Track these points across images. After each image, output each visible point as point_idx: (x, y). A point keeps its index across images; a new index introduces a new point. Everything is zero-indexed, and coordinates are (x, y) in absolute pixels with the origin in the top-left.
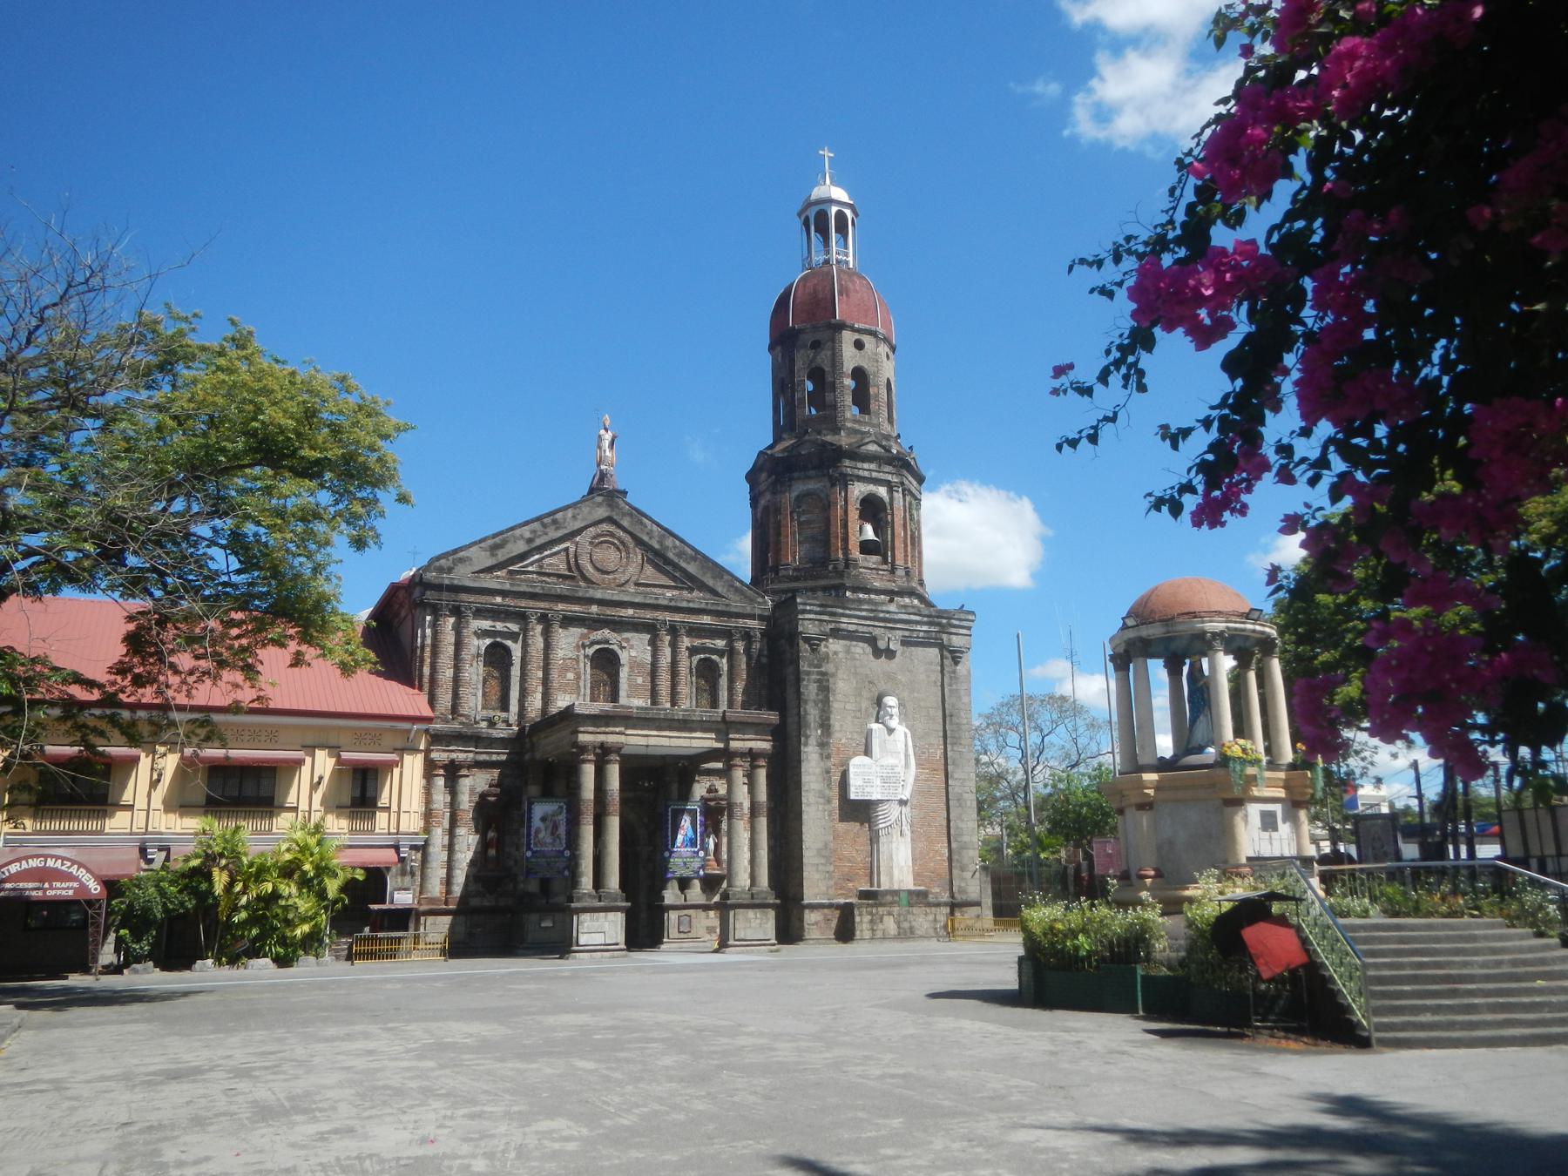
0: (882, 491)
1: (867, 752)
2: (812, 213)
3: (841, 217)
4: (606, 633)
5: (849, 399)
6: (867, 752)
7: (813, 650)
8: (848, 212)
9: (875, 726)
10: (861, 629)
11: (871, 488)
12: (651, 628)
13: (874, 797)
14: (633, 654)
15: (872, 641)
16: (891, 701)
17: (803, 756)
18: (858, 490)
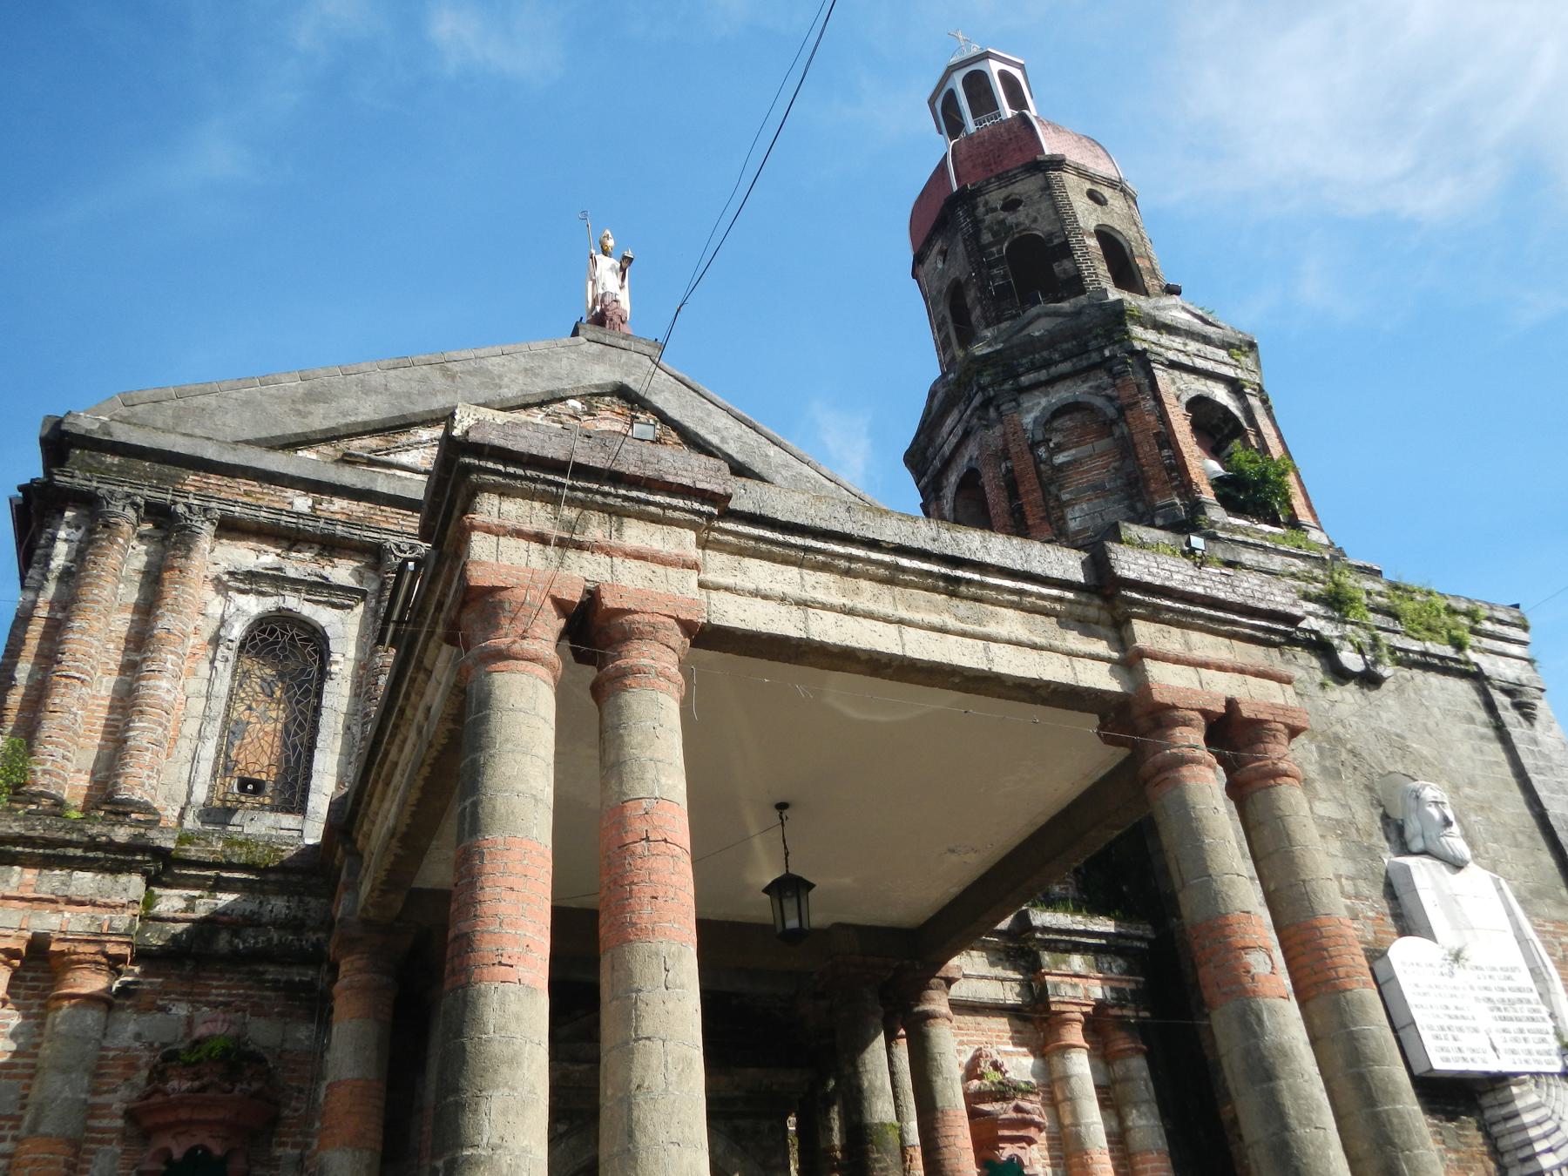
0: (1221, 395)
5: (1102, 269)
8: (1017, 73)
9: (1410, 861)
13: (1493, 1065)
15: (1322, 648)
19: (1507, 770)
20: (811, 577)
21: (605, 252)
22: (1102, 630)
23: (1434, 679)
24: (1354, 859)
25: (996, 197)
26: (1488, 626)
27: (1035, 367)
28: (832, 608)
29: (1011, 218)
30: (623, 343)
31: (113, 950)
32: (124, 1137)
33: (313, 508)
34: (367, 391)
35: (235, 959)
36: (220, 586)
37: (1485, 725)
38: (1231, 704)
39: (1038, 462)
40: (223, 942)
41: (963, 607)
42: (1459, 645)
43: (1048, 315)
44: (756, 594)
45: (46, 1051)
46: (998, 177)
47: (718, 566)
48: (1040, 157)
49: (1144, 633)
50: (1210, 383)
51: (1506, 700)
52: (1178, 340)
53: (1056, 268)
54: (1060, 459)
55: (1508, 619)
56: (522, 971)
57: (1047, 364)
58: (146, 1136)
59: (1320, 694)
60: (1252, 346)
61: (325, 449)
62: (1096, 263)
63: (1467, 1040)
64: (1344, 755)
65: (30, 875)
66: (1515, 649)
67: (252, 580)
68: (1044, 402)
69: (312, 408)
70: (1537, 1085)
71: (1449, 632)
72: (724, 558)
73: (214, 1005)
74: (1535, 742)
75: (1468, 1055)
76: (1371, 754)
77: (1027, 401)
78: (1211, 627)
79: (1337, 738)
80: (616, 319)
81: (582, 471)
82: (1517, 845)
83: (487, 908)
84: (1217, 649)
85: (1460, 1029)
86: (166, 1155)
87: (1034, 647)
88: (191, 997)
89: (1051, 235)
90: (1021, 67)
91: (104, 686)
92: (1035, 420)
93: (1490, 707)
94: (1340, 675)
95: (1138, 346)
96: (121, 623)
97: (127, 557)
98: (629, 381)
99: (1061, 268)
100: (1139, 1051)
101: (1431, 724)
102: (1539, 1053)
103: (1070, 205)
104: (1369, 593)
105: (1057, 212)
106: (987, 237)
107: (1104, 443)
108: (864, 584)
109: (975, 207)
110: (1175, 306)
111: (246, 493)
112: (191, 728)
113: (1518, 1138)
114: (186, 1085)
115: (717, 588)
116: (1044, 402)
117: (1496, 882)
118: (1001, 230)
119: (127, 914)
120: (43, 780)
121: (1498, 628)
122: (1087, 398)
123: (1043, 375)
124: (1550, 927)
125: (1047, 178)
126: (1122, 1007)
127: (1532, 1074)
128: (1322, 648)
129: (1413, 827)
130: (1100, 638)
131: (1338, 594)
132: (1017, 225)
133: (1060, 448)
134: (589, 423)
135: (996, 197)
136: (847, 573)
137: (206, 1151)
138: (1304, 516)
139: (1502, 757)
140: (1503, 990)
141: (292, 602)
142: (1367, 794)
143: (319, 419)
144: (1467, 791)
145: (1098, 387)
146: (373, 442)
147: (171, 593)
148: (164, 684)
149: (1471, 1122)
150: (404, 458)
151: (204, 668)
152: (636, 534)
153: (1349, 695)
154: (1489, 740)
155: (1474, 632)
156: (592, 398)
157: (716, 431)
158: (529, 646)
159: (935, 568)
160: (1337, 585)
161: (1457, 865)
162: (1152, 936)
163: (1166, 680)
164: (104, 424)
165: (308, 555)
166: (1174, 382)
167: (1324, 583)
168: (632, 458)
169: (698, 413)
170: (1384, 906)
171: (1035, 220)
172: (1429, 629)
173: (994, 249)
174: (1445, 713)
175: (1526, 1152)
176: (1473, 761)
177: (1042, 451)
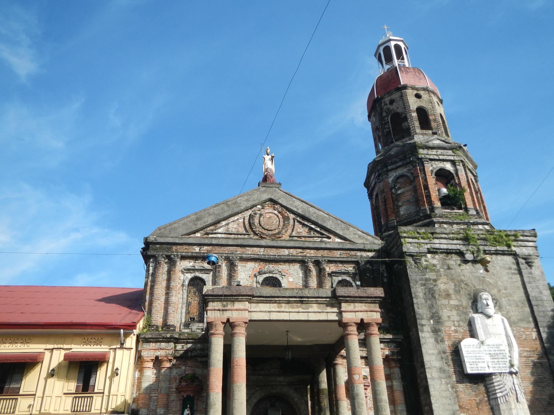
0: (448, 166)
1: (473, 334)
2: (382, 48)
3: (397, 47)
4: (271, 267)
5: (417, 124)
6: (473, 334)
7: (416, 263)
9: (476, 316)
10: (450, 247)
11: (440, 165)
12: (303, 263)
13: (487, 371)
14: (291, 280)
15: (460, 254)
16: (486, 297)
17: (422, 341)
18: (430, 167)
19: (520, 283)
20: (272, 305)
21: (268, 155)
22: (336, 305)
23: (499, 257)
24: (460, 316)
25: (387, 100)
26: (521, 238)
27: (392, 164)
28: (275, 312)
29: (391, 107)
30: (271, 186)
31: (170, 358)
32: (176, 393)
33: (200, 250)
34: (210, 215)
35: (192, 357)
36: (183, 273)
37: (515, 270)
38: (362, 320)
39: (392, 194)
40: (189, 354)
41: (304, 306)
42: (509, 246)
43: (396, 146)
44: (260, 311)
45: (161, 377)
47: (254, 307)
48: (399, 86)
49: (345, 306)
50: (445, 163)
51: (523, 261)
52: (435, 151)
53: (403, 126)
54: (399, 192)
55: (529, 235)
56: (216, 390)
57: (396, 162)
58: (180, 392)
59: (458, 268)
60: (460, 147)
61: (202, 232)
62: (415, 122)
63: (480, 365)
64: (463, 285)
65: (154, 344)
66: (531, 244)
67: (188, 270)
68: (395, 174)
69: (198, 222)
70: (500, 375)
71: (506, 242)
72: (255, 305)
73: (189, 366)
74: (531, 273)
75: (480, 369)
76: (472, 284)
78: (361, 302)
79: (462, 281)
80: (270, 177)
81: (226, 296)
82: (517, 306)
83: (211, 380)
84: (361, 307)
85: (479, 362)
86: (183, 396)
87: (319, 312)
88: (185, 365)
90: (402, 41)
91: (163, 299)
93: (518, 264)
94: (466, 262)
95: (420, 156)
96: (164, 284)
97: (164, 268)
98: (273, 197)
99: (404, 125)
100: (397, 366)
101: (495, 272)
102: (503, 367)
103: (408, 102)
104: (478, 235)
105: (404, 105)
106: (384, 114)
107: (411, 187)
108: (283, 305)
109: (381, 103)
110: (435, 139)
111: (186, 249)
112: (180, 306)
113: (493, 389)
114: (185, 384)
115: (253, 312)
117: (503, 320)
118: (389, 111)
119: (171, 351)
120: (154, 322)
121: (525, 238)
122: (406, 173)
123: (394, 166)
124: (523, 330)
125: (402, 93)
126: (393, 356)
127: (499, 373)
128: (460, 254)
129: (479, 305)
130: (335, 307)
131: (467, 237)
132: (393, 109)
133: (399, 188)
134: (263, 211)
135: (387, 100)
136: (279, 303)
137: (190, 396)
138: (470, 205)
139: (519, 279)
140: (495, 351)
141: (197, 274)
142: (468, 296)
143: (199, 226)
144: (503, 291)
145: (409, 170)
146: (212, 228)
147: (173, 277)
148: (173, 298)
149: (482, 385)
150: (220, 231)
151: (181, 291)
152: (238, 305)
153: (469, 266)
154: (515, 274)
155: (515, 240)
156: (263, 204)
157: (296, 206)
158: (217, 332)
159: (297, 299)
160: (467, 234)
161: (489, 317)
162: (402, 338)
163: (347, 317)
164: (155, 238)
165: (200, 261)
166: (432, 166)
167: (463, 234)
168: (235, 291)
169: (291, 202)
170: (467, 328)
171: (398, 108)
172: (499, 242)
173: (386, 118)
174: (501, 268)
175: (494, 392)
176: (508, 282)
177: (393, 191)
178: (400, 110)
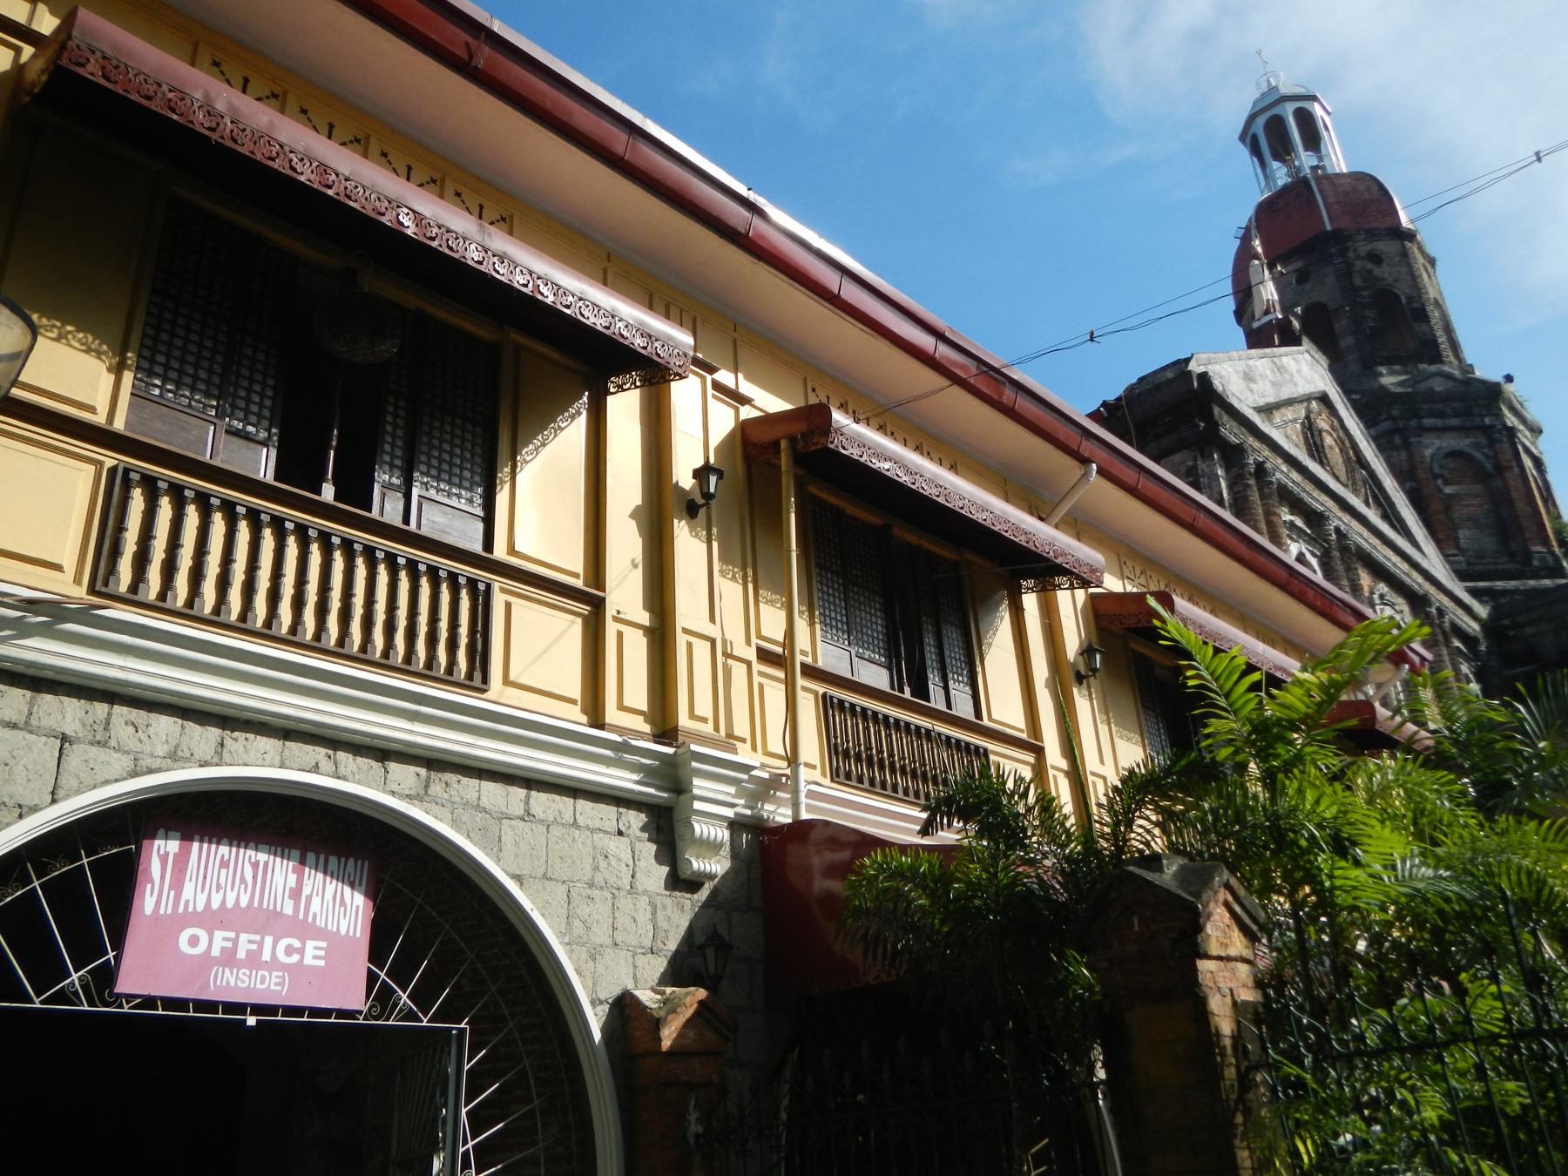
27: (1432, 415)
29: (1377, 271)
46: (1367, 231)
54: (1448, 490)
57: (1442, 415)
77: (1426, 440)
89: (1410, 299)
92: (1433, 456)
99: (1420, 328)
106: (1358, 281)
107: (1477, 488)
109: (1346, 250)
116: (1437, 443)
122: (1470, 451)
123: (1439, 422)
132: (1383, 279)
133: (1447, 483)
135: (1364, 248)
171: (1396, 280)
177: (1440, 482)
178: (1402, 290)
